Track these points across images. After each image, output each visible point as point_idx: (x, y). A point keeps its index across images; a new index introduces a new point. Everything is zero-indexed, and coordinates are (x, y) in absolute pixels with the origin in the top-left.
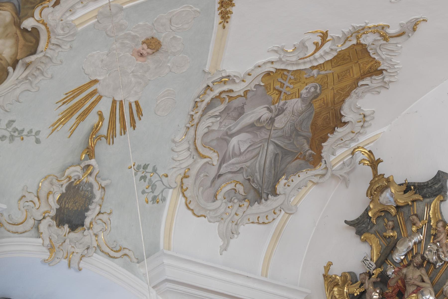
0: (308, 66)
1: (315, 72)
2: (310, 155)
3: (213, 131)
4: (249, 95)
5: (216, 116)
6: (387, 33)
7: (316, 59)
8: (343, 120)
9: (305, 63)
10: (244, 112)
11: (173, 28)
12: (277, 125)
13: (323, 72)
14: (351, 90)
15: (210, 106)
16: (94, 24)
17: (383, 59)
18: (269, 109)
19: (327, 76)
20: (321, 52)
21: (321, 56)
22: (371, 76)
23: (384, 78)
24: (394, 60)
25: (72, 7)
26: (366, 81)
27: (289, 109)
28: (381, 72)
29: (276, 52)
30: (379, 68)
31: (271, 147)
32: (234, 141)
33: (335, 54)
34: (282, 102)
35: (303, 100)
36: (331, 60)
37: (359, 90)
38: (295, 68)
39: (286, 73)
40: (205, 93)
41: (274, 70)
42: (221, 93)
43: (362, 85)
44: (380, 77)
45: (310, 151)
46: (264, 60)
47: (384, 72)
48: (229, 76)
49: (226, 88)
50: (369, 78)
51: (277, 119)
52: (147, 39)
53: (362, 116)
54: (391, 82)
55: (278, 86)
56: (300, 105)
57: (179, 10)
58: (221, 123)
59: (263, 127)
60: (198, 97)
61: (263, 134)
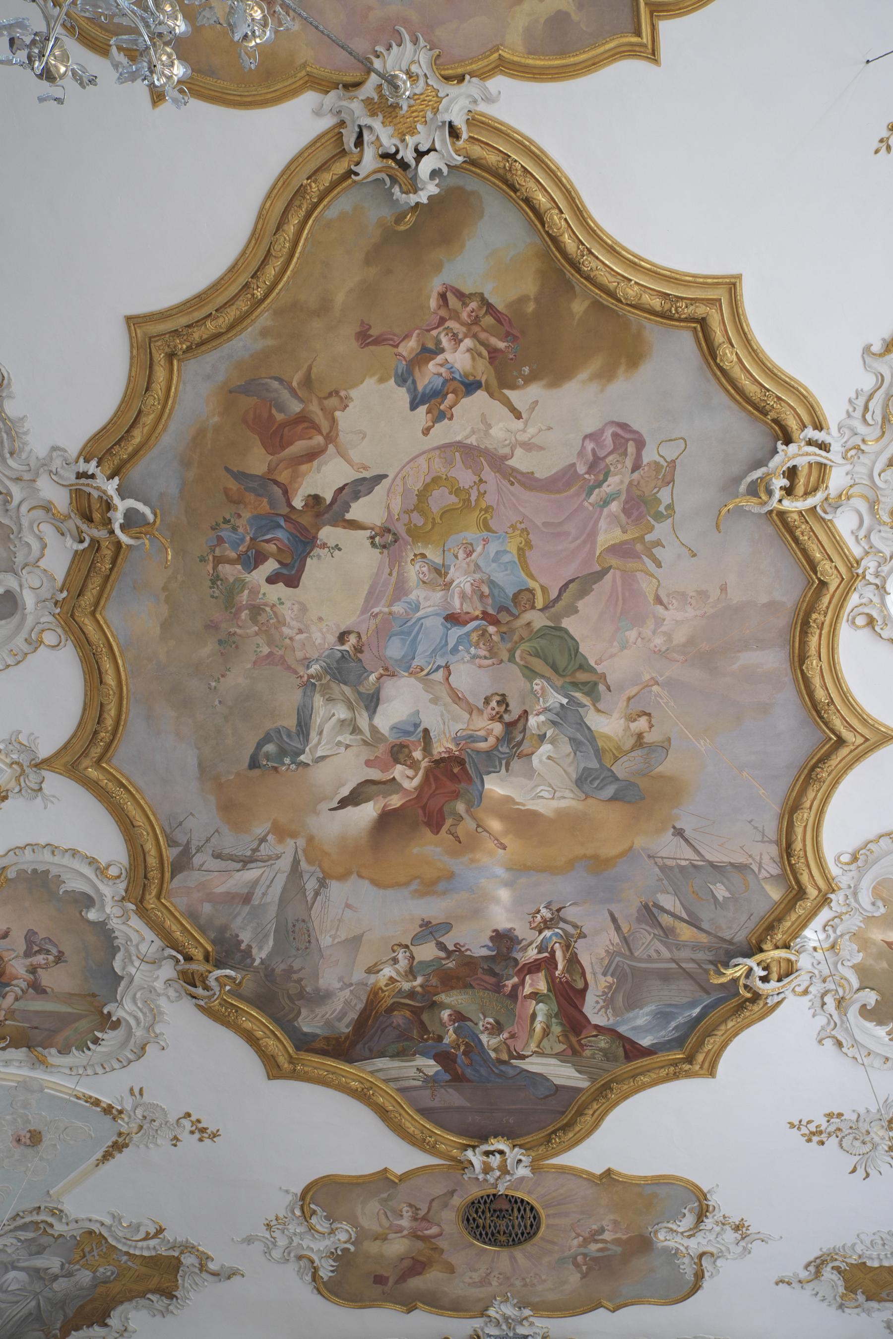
0: (125, 1249)
1: (125, 1258)
2: (55, 1336)
3: (5, 1252)
4: (60, 1240)
5: (19, 1240)
6: (206, 1265)
7: (135, 1247)
8: (108, 1321)
9: (125, 1244)
10: (42, 1253)
11: (61, 1136)
12: (56, 1286)
13: (129, 1263)
14: (136, 1297)
15: (24, 1227)
16: (11, 1087)
17: (183, 1287)
18: (62, 1265)
19: (130, 1268)
20: (145, 1244)
21: (142, 1248)
22: (161, 1295)
23: (170, 1305)
24: (192, 1295)
25: (11, 1060)
26: (154, 1297)
27: (77, 1278)
28: (171, 1297)
29: (114, 1217)
30: (174, 1293)
31: (33, 1303)
32: (12, 1274)
33: (153, 1254)
34: (77, 1267)
35: (94, 1278)
36: (145, 1257)
37: (142, 1302)
38: (114, 1243)
39: (103, 1242)
40: (31, 1212)
41: (98, 1232)
42: (42, 1222)
43: (149, 1299)
44: (167, 1301)
45: (57, 1331)
46: (98, 1218)
47: (175, 1299)
48: (61, 1211)
49: (50, 1220)
50: (158, 1296)
51: (61, 1280)
52: (35, 1131)
53: (123, 1329)
54: (172, 1312)
55: (87, 1249)
56: (88, 1279)
57: (79, 1124)
58: (17, 1249)
59: (44, 1279)
60: (23, 1212)
61: (38, 1286)
